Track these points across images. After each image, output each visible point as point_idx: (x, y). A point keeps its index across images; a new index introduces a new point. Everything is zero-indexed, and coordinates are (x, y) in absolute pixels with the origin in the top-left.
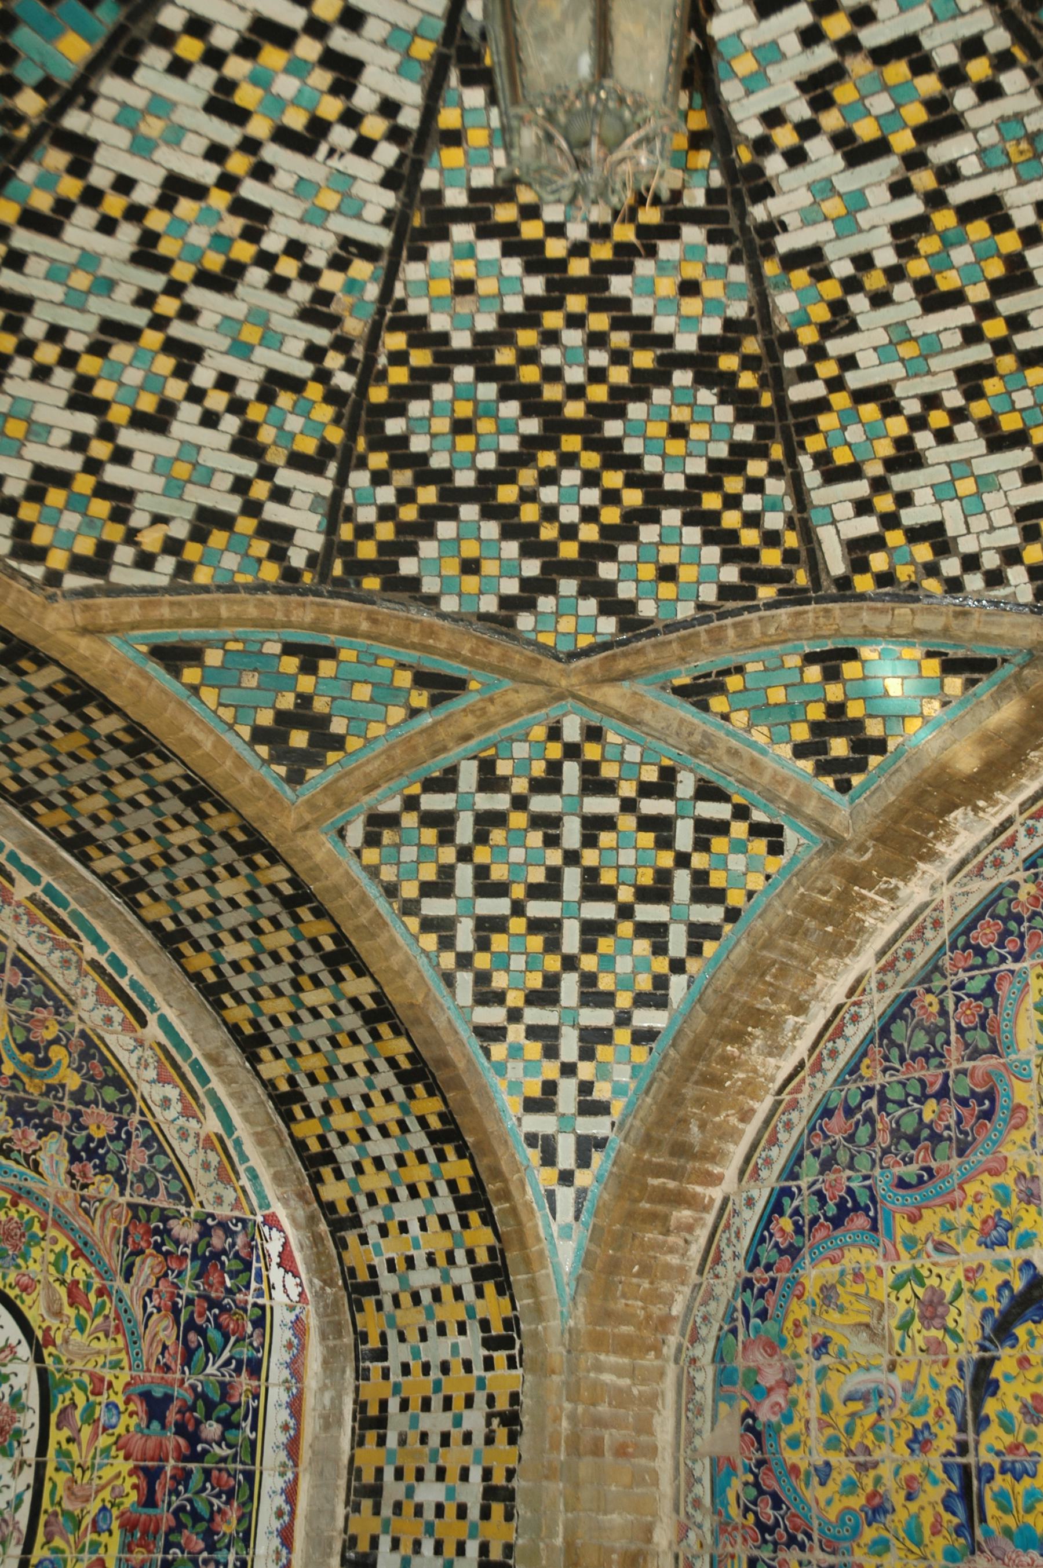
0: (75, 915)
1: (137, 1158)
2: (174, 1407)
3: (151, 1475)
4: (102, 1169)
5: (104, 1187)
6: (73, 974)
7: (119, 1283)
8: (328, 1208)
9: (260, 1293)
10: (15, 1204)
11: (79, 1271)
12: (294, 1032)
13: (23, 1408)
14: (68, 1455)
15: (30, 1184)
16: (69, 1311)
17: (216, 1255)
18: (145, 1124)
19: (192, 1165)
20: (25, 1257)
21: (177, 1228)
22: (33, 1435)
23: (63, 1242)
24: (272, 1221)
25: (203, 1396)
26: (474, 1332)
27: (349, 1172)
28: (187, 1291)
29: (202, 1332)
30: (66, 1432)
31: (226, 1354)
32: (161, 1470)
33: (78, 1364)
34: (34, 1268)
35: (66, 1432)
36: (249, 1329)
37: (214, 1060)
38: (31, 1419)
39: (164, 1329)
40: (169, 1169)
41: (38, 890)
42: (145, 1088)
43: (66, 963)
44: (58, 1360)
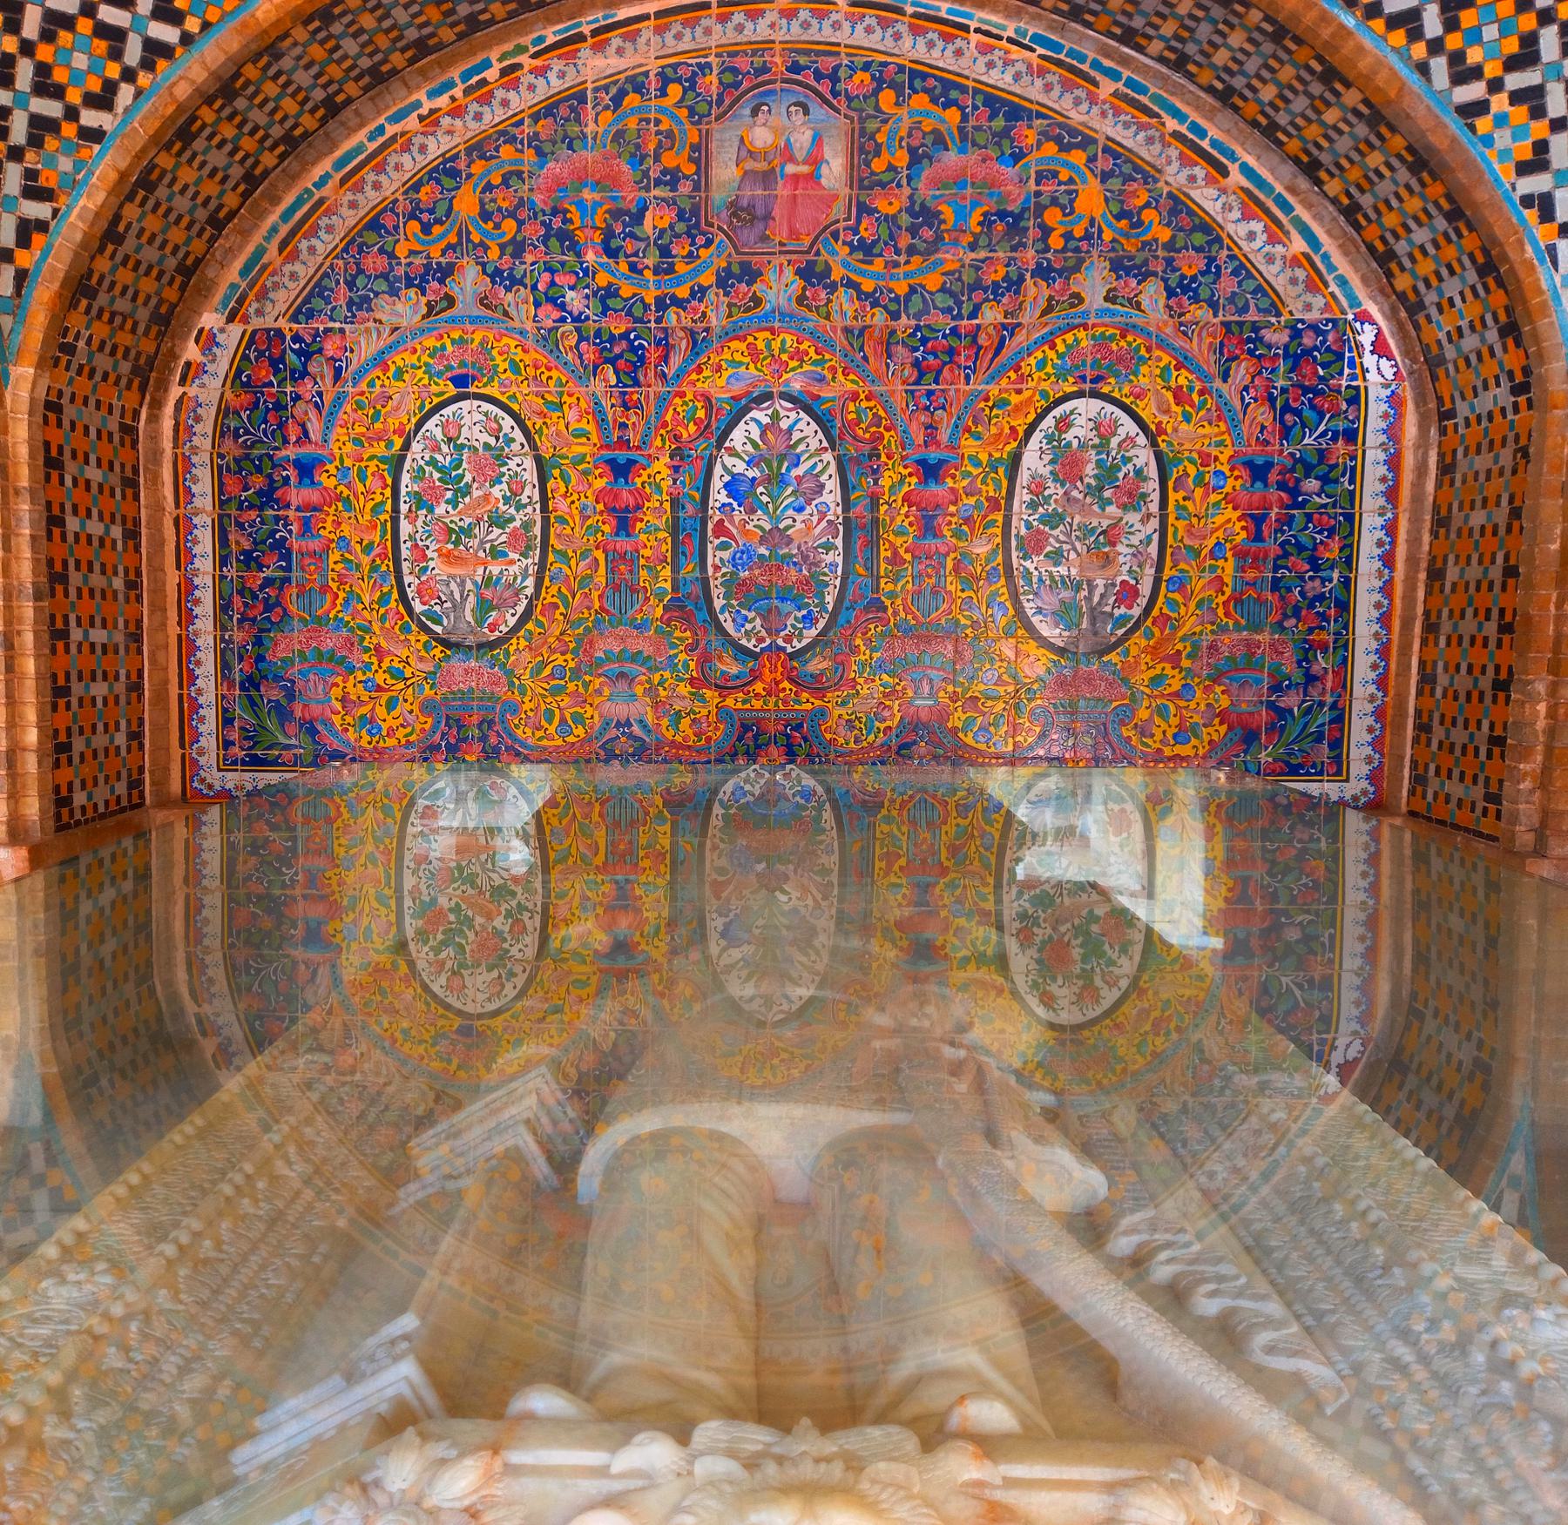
0: (1156, 99)
1: (1227, 285)
2: (1276, 469)
3: (1259, 520)
4: (1196, 299)
5: (1201, 313)
6: (1157, 147)
7: (1218, 383)
8: (1402, 297)
9: (1353, 377)
10: (1123, 336)
11: (1183, 379)
12: (1332, 150)
13: (1146, 479)
14: (1185, 508)
15: (1134, 320)
16: (1174, 408)
17: (1308, 352)
18: (1232, 257)
19: (1280, 283)
20: (1135, 374)
21: (1268, 335)
22: (1156, 496)
23: (1166, 359)
24: (1364, 317)
25: (1301, 460)
26: (1505, 384)
27: (1407, 263)
28: (1280, 383)
29: (1298, 413)
30: (1182, 494)
31: (1322, 428)
32: (1264, 517)
33: (1188, 446)
34: (1144, 382)
35: (1182, 494)
36: (1344, 406)
37: (1292, 190)
38: (1152, 486)
39: (1262, 415)
40: (1258, 289)
41: (1120, 85)
42: (1231, 228)
43: (1150, 140)
44: (1170, 444)
